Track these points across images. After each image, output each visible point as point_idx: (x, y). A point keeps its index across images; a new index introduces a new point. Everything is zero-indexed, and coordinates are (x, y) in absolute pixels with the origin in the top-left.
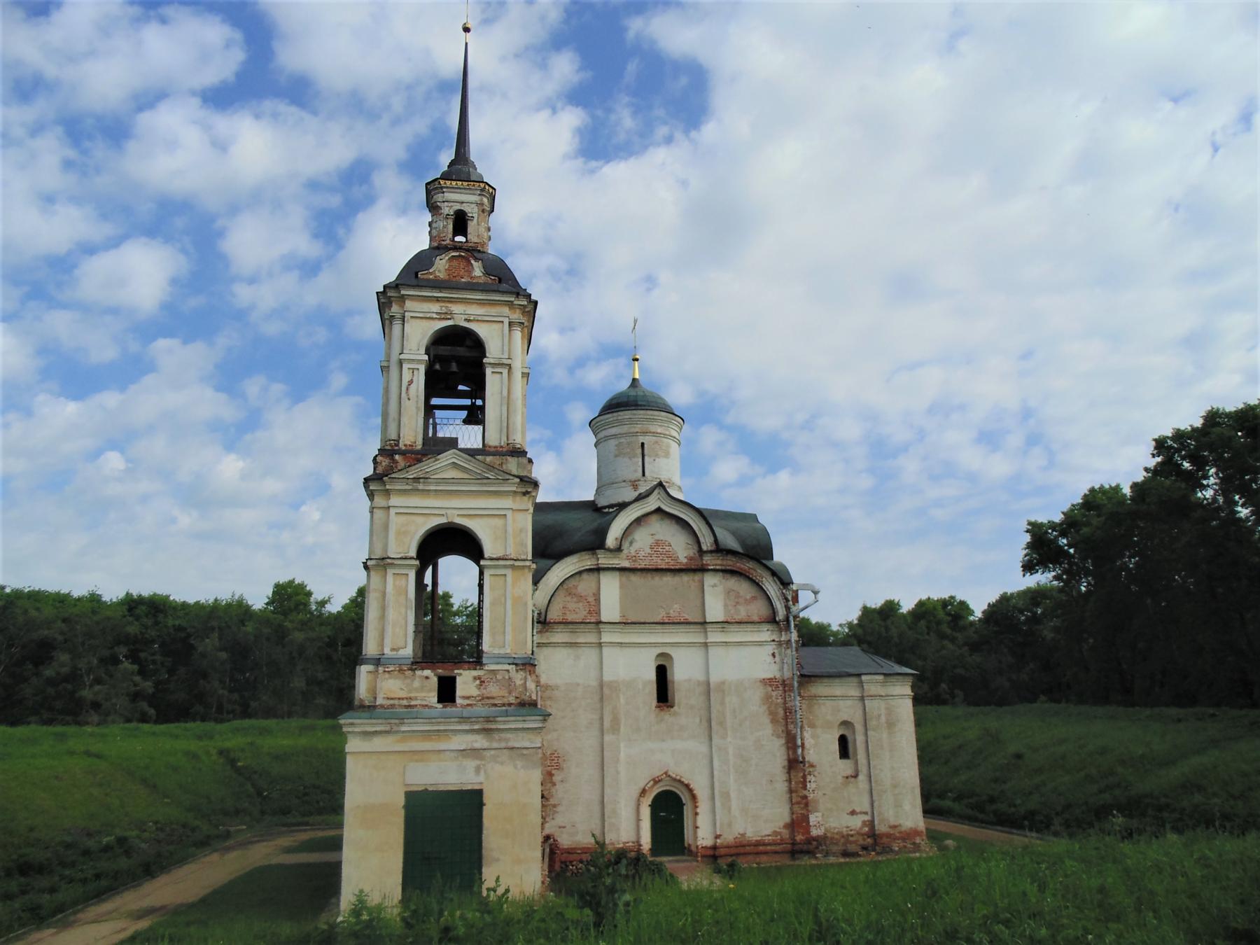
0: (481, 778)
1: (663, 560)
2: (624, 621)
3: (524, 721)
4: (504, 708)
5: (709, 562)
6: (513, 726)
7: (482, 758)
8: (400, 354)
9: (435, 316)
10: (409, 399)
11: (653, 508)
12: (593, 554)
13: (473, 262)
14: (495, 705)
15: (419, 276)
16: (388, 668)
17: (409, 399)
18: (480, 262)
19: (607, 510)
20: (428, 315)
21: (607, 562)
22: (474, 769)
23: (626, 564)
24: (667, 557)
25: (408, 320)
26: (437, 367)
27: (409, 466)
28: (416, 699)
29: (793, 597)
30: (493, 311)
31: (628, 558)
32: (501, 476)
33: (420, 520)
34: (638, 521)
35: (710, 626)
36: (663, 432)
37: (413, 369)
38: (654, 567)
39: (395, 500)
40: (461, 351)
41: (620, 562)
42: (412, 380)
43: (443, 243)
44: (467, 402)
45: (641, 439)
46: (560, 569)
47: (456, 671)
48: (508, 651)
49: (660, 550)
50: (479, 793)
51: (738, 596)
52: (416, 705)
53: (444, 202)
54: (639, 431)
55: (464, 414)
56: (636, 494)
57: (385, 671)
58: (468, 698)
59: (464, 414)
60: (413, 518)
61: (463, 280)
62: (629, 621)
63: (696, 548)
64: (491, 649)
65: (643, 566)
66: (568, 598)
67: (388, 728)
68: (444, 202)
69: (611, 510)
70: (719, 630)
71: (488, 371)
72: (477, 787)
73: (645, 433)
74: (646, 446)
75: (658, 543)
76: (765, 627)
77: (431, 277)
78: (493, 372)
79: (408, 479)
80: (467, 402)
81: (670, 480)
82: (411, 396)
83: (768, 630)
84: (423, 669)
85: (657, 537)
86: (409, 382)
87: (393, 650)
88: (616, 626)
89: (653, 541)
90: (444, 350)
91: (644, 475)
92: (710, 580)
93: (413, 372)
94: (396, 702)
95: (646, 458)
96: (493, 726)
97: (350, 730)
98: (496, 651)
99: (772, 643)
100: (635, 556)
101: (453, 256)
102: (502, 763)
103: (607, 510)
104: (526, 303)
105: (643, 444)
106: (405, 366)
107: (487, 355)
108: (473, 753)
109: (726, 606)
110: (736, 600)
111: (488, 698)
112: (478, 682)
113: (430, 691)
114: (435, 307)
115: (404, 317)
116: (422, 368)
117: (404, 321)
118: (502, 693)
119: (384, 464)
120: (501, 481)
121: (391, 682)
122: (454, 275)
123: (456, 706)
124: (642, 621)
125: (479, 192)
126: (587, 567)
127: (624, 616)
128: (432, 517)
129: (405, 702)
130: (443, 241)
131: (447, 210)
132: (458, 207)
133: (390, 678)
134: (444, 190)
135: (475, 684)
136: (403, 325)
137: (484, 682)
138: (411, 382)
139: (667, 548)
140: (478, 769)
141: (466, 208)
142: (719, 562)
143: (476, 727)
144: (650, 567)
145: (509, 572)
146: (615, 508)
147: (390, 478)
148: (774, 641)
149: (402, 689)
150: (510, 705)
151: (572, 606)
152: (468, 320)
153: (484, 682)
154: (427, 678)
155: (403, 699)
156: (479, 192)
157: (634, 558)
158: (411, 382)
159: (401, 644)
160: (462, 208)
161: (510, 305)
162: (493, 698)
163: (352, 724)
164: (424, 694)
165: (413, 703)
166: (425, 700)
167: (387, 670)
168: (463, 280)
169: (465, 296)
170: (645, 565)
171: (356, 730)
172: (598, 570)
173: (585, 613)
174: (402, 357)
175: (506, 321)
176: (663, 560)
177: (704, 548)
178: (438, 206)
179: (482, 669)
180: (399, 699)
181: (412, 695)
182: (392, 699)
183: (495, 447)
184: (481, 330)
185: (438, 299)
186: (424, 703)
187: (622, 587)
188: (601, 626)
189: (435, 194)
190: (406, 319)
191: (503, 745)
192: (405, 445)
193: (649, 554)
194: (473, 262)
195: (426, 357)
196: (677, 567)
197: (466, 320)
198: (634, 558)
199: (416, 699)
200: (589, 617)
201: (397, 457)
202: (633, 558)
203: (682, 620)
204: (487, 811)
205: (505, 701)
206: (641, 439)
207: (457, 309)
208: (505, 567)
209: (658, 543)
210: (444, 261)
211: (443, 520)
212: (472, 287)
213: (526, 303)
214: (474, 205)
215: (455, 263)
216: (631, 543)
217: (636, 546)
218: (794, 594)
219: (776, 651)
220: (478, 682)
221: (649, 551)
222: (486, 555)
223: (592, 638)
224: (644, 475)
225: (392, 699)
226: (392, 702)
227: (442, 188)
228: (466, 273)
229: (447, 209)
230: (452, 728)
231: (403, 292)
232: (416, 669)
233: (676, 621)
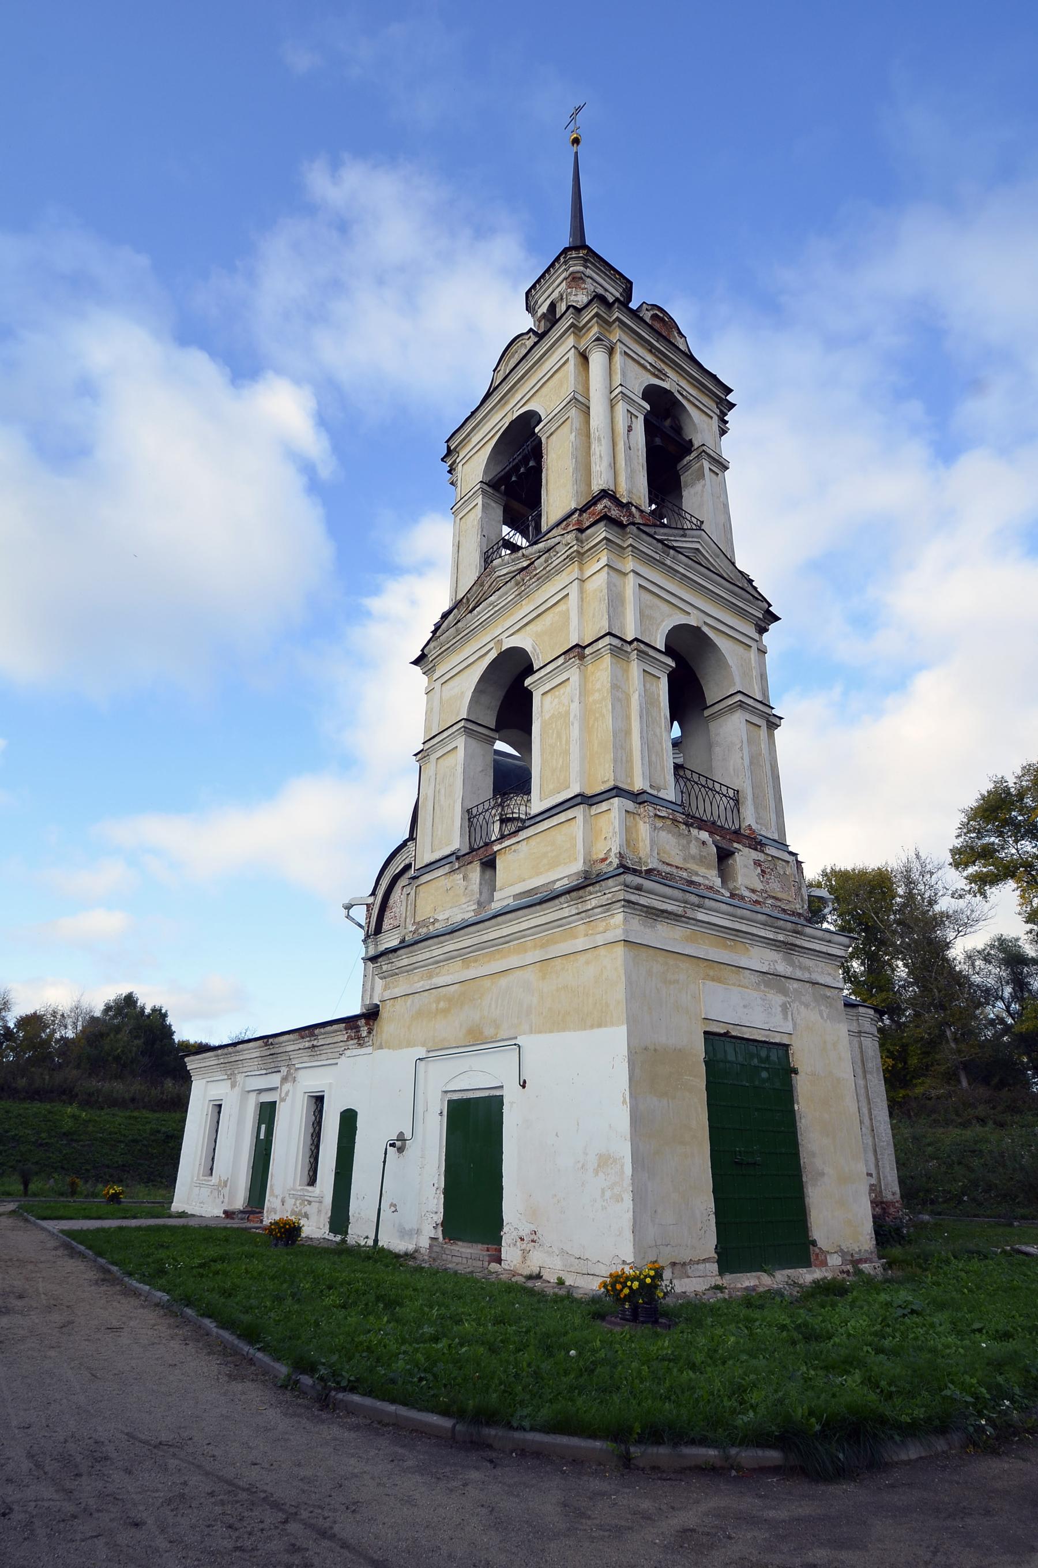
0: (788, 1027)
3: (829, 941)
6: (818, 947)
7: (784, 992)
8: (611, 393)
9: (649, 367)
16: (659, 810)
18: (683, 339)
20: (642, 362)
22: (780, 1009)
28: (697, 874)
33: (665, 607)
37: (632, 413)
47: (736, 845)
50: (786, 1047)
52: (700, 884)
57: (656, 815)
58: (753, 891)
60: (657, 601)
67: (680, 911)
72: (786, 1041)
78: (710, 468)
84: (700, 829)
96: (798, 942)
101: (656, 314)
102: (807, 1006)
108: (771, 979)
115: (612, 348)
120: (751, 597)
128: (677, 611)
138: (630, 429)
140: (785, 1008)
143: (781, 937)
154: (704, 843)
155: (681, 868)
163: (639, 888)
165: (695, 878)
166: (708, 879)
167: (658, 813)
169: (681, 363)
171: (643, 901)
178: (581, 278)
180: (677, 867)
182: (668, 864)
191: (806, 976)
197: (678, 391)
201: (633, 509)
204: (803, 1086)
225: (668, 864)
226: (668, 869)
230: (755, 931)
232: (692, 825)
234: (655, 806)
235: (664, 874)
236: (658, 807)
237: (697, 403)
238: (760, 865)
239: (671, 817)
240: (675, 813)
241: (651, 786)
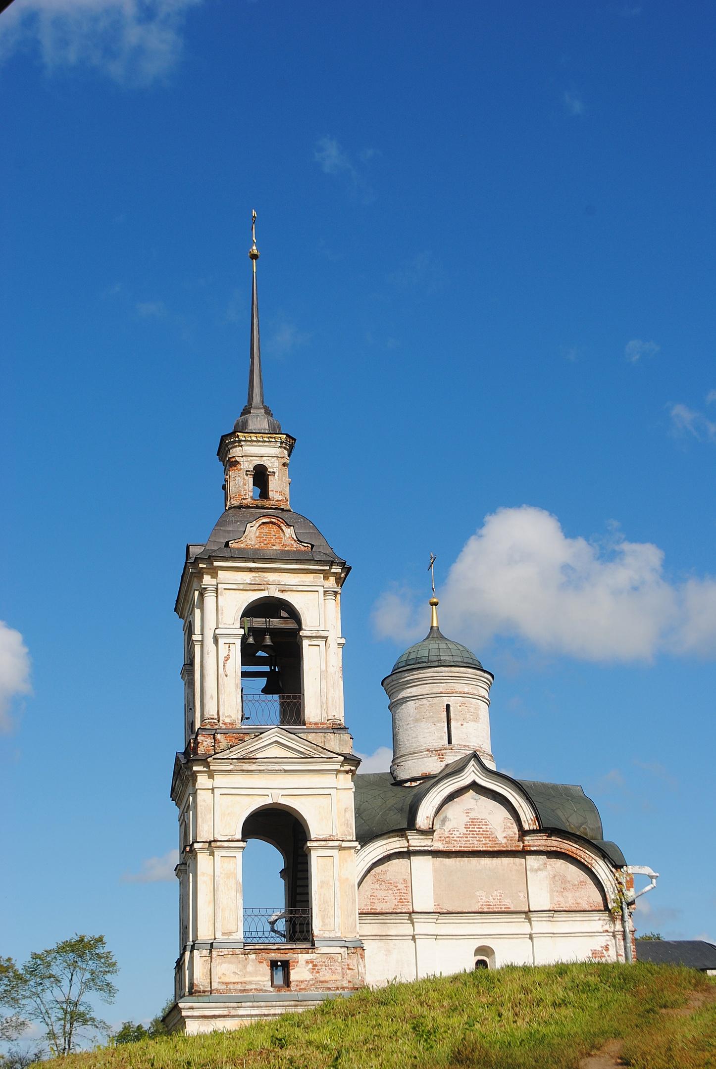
1: (480, 841)
2: (439, 910)
4: (338, 992)
5: (531, 843)
10: (226, 676)
11: (467, 781)
12: (402, 836)
13: (284, 528)
14: (329, 989)
15: (230, 545)
16: (221, 952)
17: (226, 676)
19: (408, 784)
21: (418, 845)
23: (439, 846)
24: (484, 837)
25: (221, 592)
26: (251, 640)
27: (232, 746)
29: (627, 881)
30: (309, 578)
31: (440, 839)
32: (325, 754)
34: (451, 797)
35: (535, 915)
36: (471, 691)
38: (470, 849)
39: (220, 780)
40: (275, 623)
41: (432, 844)
42: (228, 655)
43: (244, 501)
44: (267, 669)
45: (446, 700)
46: (367, 852)
48: (338, 935)
49: (476, 829)
51: (564, 881)
52: (251, 990)
53: (242, 457)
54: (443, 691)
55: (263, 682)
56: (443, 764)
59: (263, 682)
61: (274, 548)
62: (445, 911)
63: (515, 829)
64: (322, 932)
65: (458, 849)
66: (377, 886)
68: (242, 457)
69: (414, 784)
70: (544, 919)
71: (306, 643)
73: (450, 693)
74: (451, 708)
75: (473, 821)
76: (596, 916)
77: (242, 545)
79: (232, 759)
80: (267, 669)
81: (480, 747)
82: (228, 673)
83: (599, 920)
85: (472, 815)
86: (225, 657)
87: (224, 934)
88: (430, 916)
89: (467, 819)
90: (259, 622)
91: (450, 742)
92: (533, 861)
93: (229, 647)
94: (231, 986)
95: (453, 723)
97: (189, 1013)
98: (327, 935)
99: (605, 934)
100: (448, 837)
101: (263, 523)
103: (408, 784)
104: (340, 571)
105: (448, 706)
106: (221, 641)
107: (303, 627)
109: (552, 891)
110: (563, 886)
111: (322, 982)
112: (310, 966)
113: (264, 975)
114: (248, 577)
116: (238, 642)
117: (217, 594)
118: (334, 977)
119: (205, 743)
121: (225, 966)
122: (265, 542)
123: (291, 991)
124: (460, 910)
125: (279, 445)
126: (397, 850)
127: (438, 905)
129: (239, 987)
130: (244, 499)
131: (247, 465)
132: (257, 461)
133: (225, 962)
134: (243, 443)
135: (308, 968)
136: (217, 597)
137: (316, 966)
138: (227, 658)
139: (484, 827)
141: (266, 462)
142: (543, 842)
144: (466, 849)
145: (335, 852)
146: (418, 782)
147: (214, 759)
148: (607, 931)
149: (235, 973)
150: (343, 988)
151: (381, 894)
152: (282, 591)
153: (316, 966)
155: (238, 983)
156: (279, 445)
157: (447, 839)
158: (227, 658)
159: (233, 929)
160: (262, 463)
161: (326, 575)
162: (326, 982)
164: (258, 978)
165: (248, 987)
166: (260, 984)
168: (274, 548)
170: (460, 847)
172: (407, 854)
173: (395, 902)
174: (217, 632)
175: (321, 590)
176: (480, 841)
177: (526, 827)
178: (236, 461)
179: (315, 952)
180: (234, 983)
181: (247, 979)
183: (316, 724)
184: (295, 600)
185: (251, 570)
186: (258, 987)
187: (435, 871)
188: (414, 916)
189: (232, 448)
190: (219, 591)
192: (225, 724)
193: (464, 834)
194: (284, 528)
195: (242, 632)
196: (496, 849)
198: (447, 839)
199: (250, 983)
200: (400, 907)
201: (219, 736)
202: (447, 840)
203: (503, 909)
205: (339, 984)
206: (446, 700)
207: (271, 577)
208: (333, 847)
209: (473, 821)
210: (254, 528)
211: (268, 801)
212: (285, 557)
213: (340, 571)
214: (274, 460)
215: (265, 529)
216: (444, 821)
217: (449, 826)
218: (628, 879)
219: (609, 943)
220: (310, 966)
221: (464, 831)
222: (313, 837)
223: (406, 929)
224: (450, 742)
227: (240, 441)
228: (278, 541)
229: (246, 464)
231: (216, 564)
233: (496, 910)
234: (218, 950)
235: (221, 991)
236: (221, 950)
237: (300, 588)
238: (312, 962)
239: (231, 953)
240: (235, 950)
241: (224, 934)
